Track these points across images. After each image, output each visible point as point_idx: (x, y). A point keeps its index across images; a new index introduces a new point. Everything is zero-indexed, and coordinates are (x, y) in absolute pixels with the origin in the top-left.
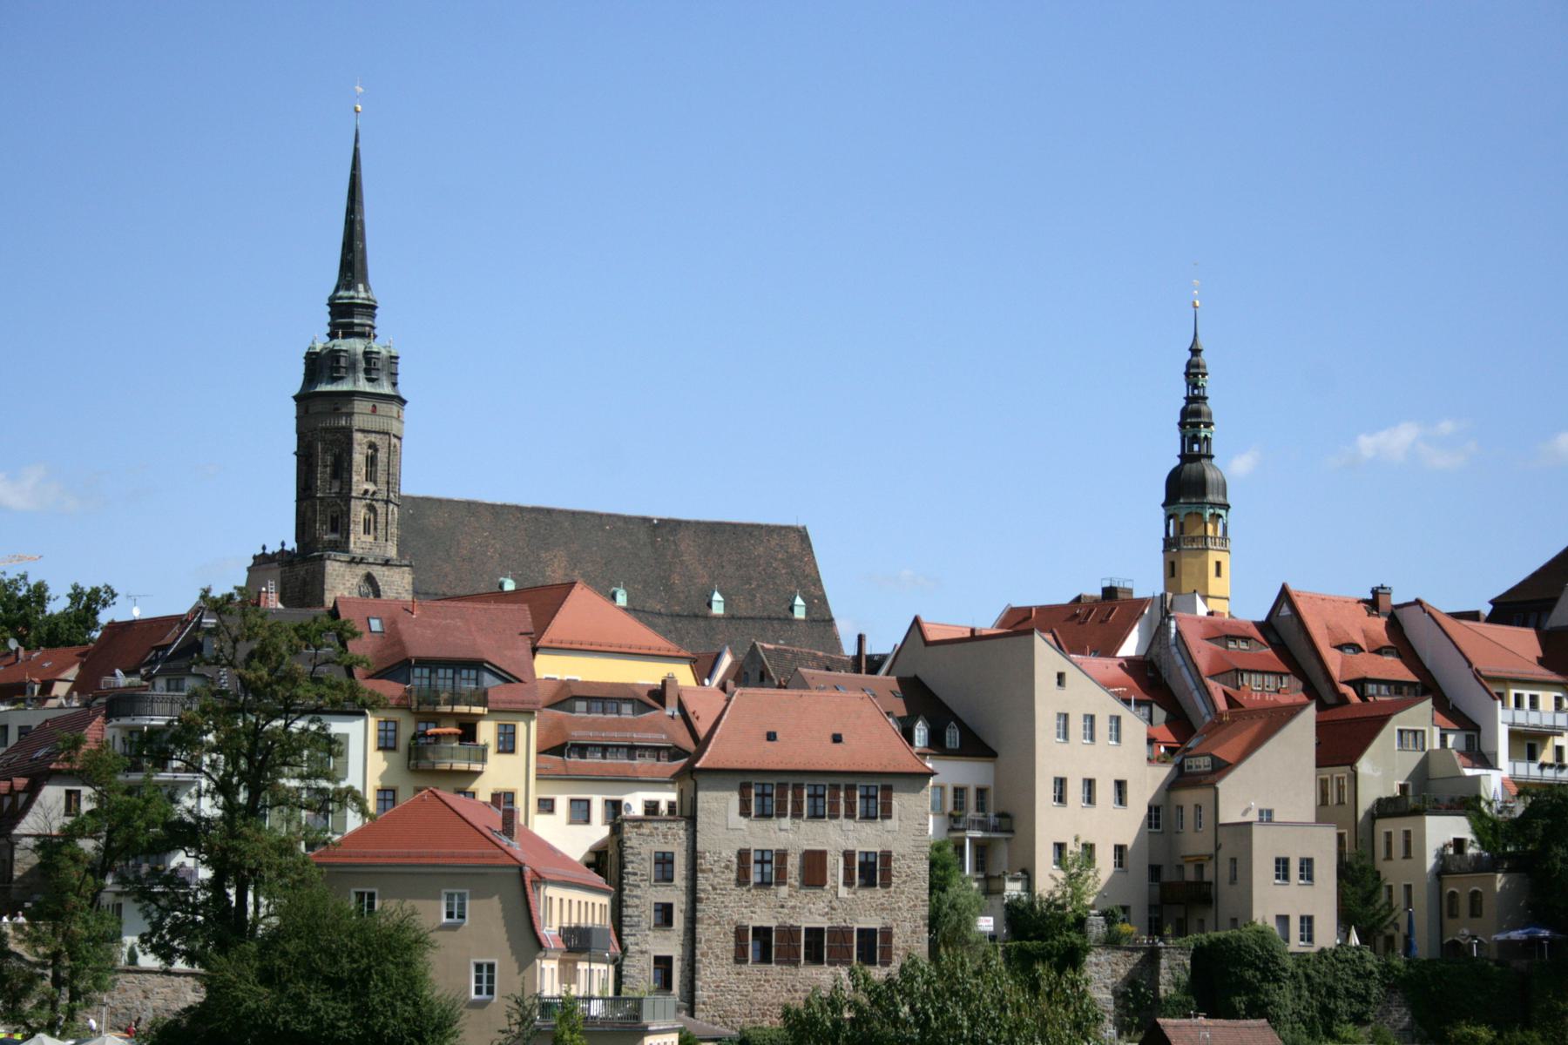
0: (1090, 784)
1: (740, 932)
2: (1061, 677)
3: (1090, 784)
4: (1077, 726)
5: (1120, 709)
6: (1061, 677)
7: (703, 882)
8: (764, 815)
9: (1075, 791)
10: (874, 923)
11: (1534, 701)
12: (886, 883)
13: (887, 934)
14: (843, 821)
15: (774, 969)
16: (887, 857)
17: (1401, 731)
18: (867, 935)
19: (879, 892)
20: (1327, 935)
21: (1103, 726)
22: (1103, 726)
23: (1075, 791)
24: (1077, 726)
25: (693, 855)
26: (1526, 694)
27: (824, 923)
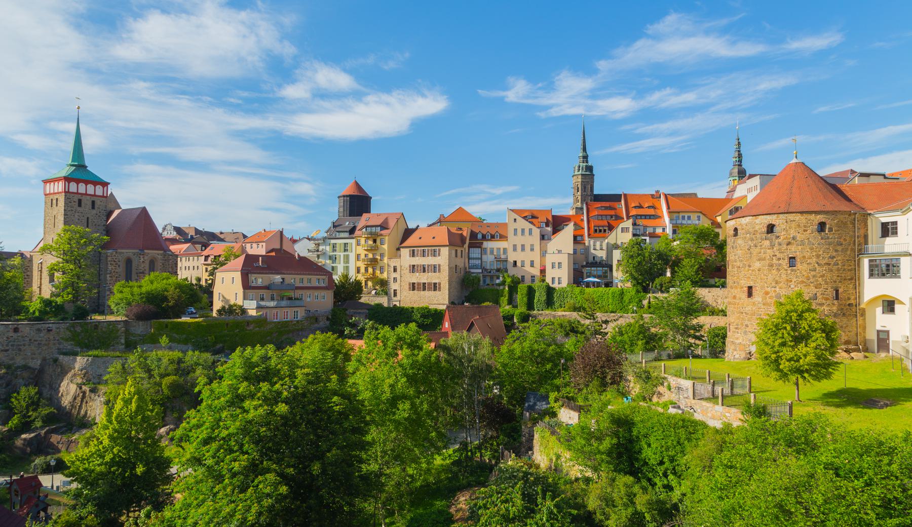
0: (523, 247)
1: (410, 284)
2: (515, 220)
3: (523, 247)
4: (519, 232)
5: (531, 226)
6: (515, 220)
7: (402, 273)
8: (413, 256)
9: (519, 248)
10: (437, 281)
11: (689, 218)
12: (439, 271)
13: (440, 284)
14: (430, 257)
15: (416, 292)
16: (439, 265)
17: (622, 228)
18: (435, 284)
19: (437, 274)
20: (564, 284)
21: (527, 232)
22: (527, 232)
23: (519, 248)
24: (519, 232)
25: (401, 267)
26: (686, 215)
27: (426, 281)
